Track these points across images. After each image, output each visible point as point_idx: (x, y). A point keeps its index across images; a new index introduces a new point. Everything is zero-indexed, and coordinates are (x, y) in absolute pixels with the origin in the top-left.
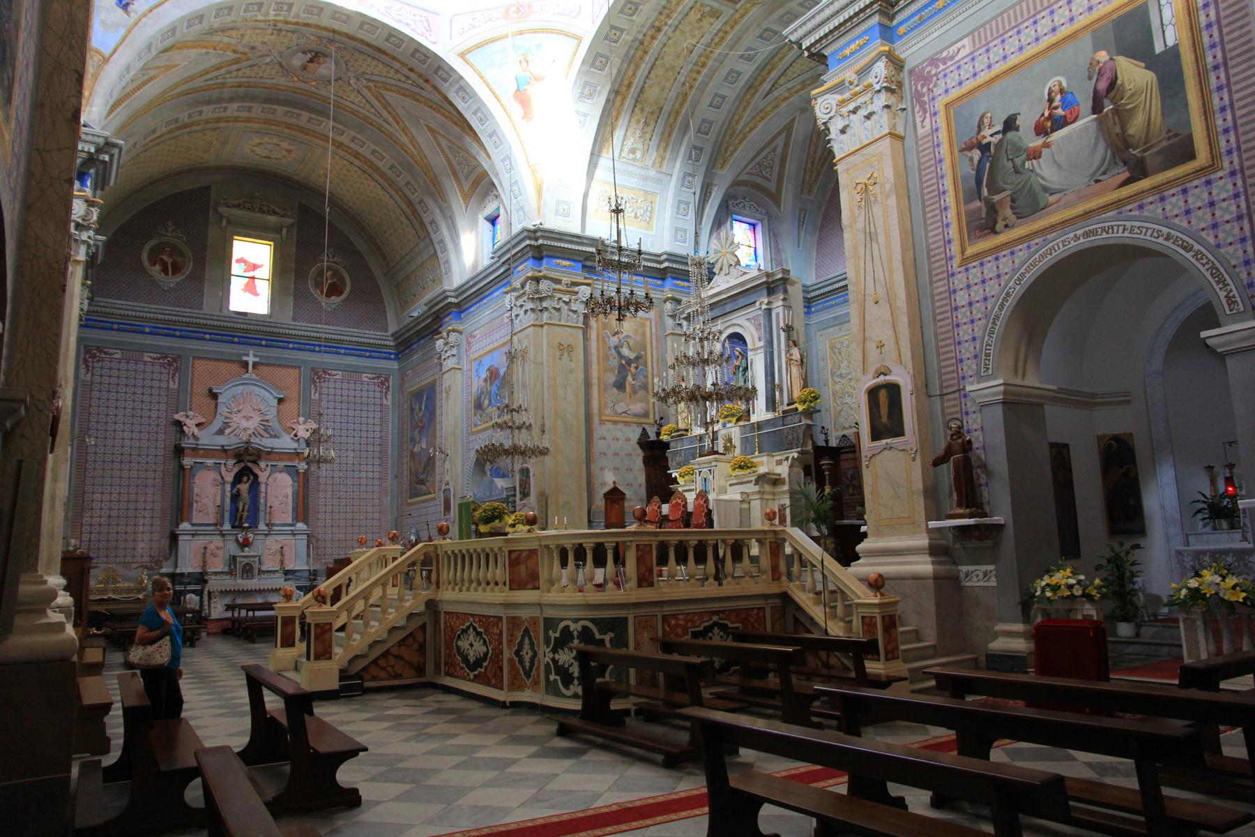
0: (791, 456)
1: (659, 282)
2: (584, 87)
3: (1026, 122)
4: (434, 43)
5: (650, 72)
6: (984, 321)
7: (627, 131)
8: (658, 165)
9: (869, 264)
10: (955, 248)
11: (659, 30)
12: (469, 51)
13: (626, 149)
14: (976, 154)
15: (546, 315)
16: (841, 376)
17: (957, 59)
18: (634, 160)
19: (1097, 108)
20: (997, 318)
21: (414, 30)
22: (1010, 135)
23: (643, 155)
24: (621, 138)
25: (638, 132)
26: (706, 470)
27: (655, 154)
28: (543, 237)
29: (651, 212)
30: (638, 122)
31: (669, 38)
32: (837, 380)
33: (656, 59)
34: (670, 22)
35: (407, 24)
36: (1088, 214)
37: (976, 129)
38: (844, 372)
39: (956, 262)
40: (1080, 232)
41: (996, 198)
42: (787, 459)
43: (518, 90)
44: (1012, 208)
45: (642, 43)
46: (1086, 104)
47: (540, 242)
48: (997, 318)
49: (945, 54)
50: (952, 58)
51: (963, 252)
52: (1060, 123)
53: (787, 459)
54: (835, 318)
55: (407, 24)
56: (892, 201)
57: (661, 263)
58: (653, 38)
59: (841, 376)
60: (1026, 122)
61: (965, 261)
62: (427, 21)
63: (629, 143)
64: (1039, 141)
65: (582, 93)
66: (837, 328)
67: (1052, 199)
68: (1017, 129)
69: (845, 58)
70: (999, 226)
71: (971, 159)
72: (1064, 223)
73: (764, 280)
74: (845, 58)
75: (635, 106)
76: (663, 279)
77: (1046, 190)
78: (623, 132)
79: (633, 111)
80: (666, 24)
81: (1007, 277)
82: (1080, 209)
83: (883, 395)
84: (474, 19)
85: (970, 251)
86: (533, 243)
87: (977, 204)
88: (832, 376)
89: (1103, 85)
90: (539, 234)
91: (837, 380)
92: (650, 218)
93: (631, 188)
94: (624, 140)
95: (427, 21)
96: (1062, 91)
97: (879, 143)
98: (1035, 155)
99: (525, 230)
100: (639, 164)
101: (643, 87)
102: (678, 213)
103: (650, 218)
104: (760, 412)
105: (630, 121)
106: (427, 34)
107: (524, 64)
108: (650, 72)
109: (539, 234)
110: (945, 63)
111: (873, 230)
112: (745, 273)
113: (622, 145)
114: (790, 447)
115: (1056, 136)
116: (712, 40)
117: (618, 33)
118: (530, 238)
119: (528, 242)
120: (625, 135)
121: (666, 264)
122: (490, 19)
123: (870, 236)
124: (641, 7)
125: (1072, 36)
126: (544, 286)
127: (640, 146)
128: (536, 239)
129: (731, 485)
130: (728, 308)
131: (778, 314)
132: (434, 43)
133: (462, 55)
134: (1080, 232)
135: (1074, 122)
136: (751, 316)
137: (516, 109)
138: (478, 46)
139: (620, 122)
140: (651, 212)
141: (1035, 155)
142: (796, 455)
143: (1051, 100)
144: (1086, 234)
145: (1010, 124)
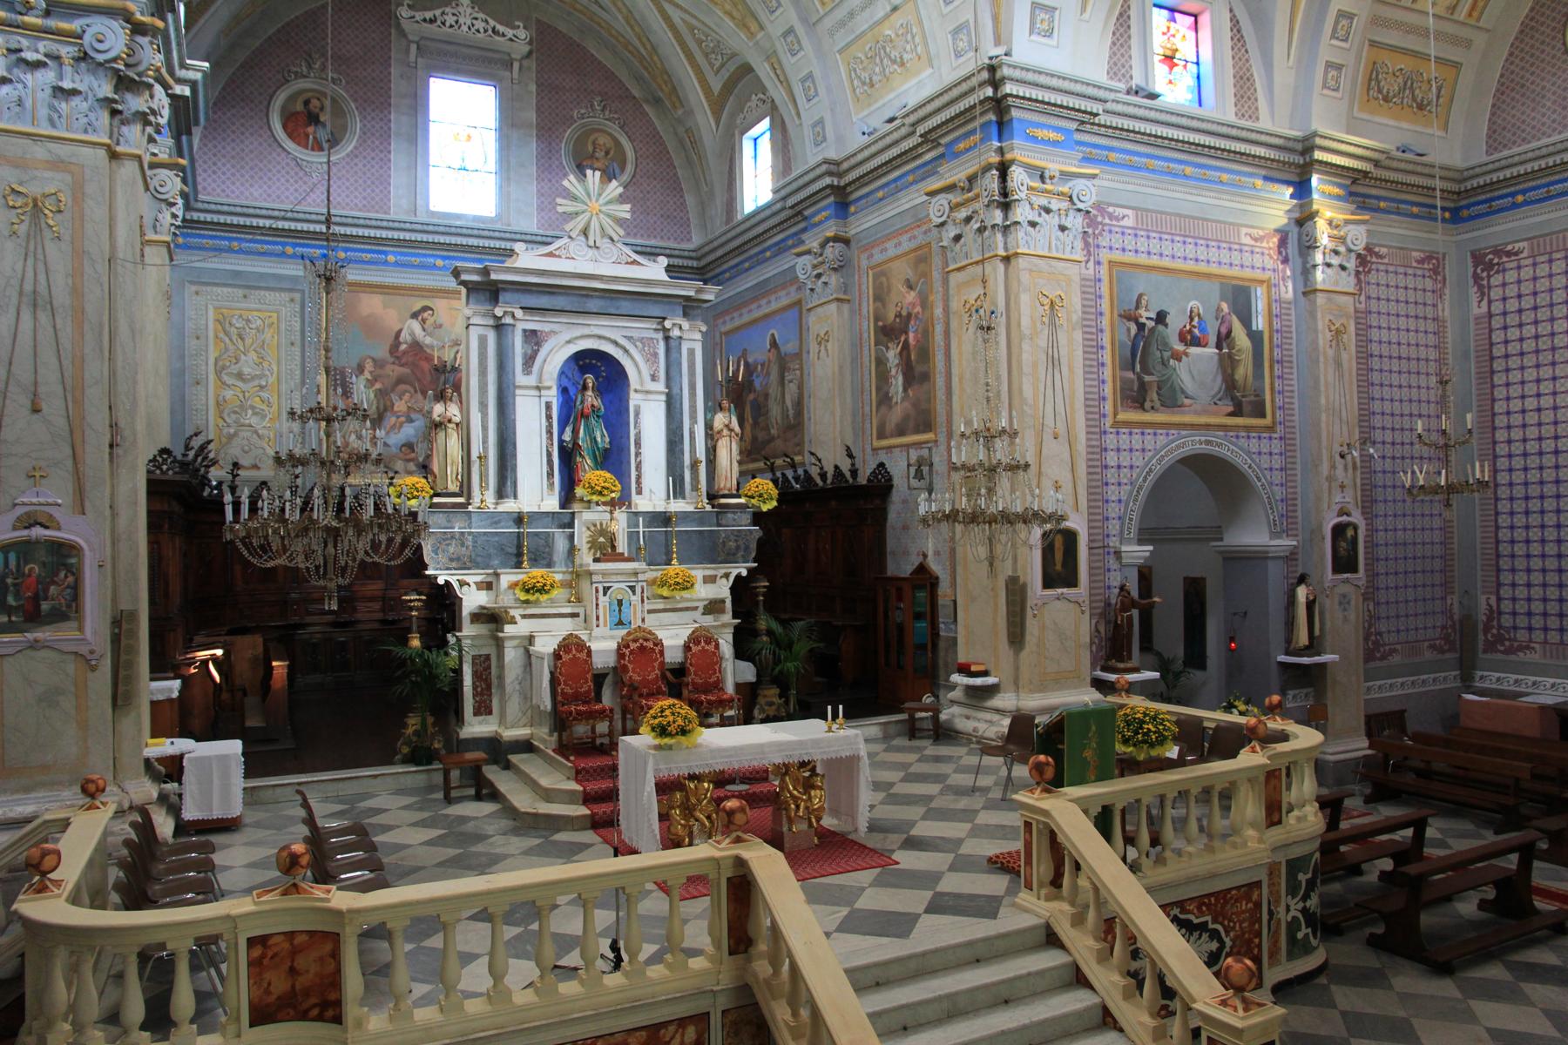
0: (734, 573)
3: (1176, 322)
6: (1128, 487)
9: (1049, 392)
10: (1108, 407)
14: (1134, 329)
16: (240, 376)
17: (1122, 223)
19: (1219, 346)
20: (1140, 488)
22: (1161, 327)
26: (623, 585)
32: (229, 381)
36: (1207, 426)
37: (1134, 304)
38: (246, 370)
39: (1109, 421)
40: (1203, 439)
41: (1147, 378)
42: (727, 576)
44: (1158, 394)
46: (1213, 339)
48: (1140, 488)
49: (1111, 209)
50: (1117, 219)
51: (1115, 414)
52: (1197, 342)
53: (727, 576)
54: (237, 274)
56: (1078, 336)
59: (240, 376)
60: (1176, 322)
61: (1116, 424)
64: (1180, 347)
66: (240, 292)
67: (1187, 401)
68: (1166, 325)
69: (1034, 139)
70: (1147, 405)
71: (1129, 330)
72: (1193, 426)
74: (1034, 139)
77: (1183, 391)
81: (1150, 454)
82: (1203, 420)
83: (1059, 542)
85: (1121, 416)
87: (1130, 375)
88: (218, 373)
89: (1224, 330)
91: (229, 381)
96: (1199, 315)
97: (1069, 265)
98: (1177, 357)
104: (653, 494)
110: (1111, 219)
111: (1056, 356)
114: (730, 558)
115: (1193, 350)
123: (1054, 362)
125: (1208, 276)
129: (650, 612)
130: (593, 305)
131: (691, 352)
134: (1203, 439)
135: (1204, 346)
136: (635, 334)
141: (1177, 357)
142: (744, 573)
143: (1192, 319)
144: (1208, 442)
145: (1161, 318)
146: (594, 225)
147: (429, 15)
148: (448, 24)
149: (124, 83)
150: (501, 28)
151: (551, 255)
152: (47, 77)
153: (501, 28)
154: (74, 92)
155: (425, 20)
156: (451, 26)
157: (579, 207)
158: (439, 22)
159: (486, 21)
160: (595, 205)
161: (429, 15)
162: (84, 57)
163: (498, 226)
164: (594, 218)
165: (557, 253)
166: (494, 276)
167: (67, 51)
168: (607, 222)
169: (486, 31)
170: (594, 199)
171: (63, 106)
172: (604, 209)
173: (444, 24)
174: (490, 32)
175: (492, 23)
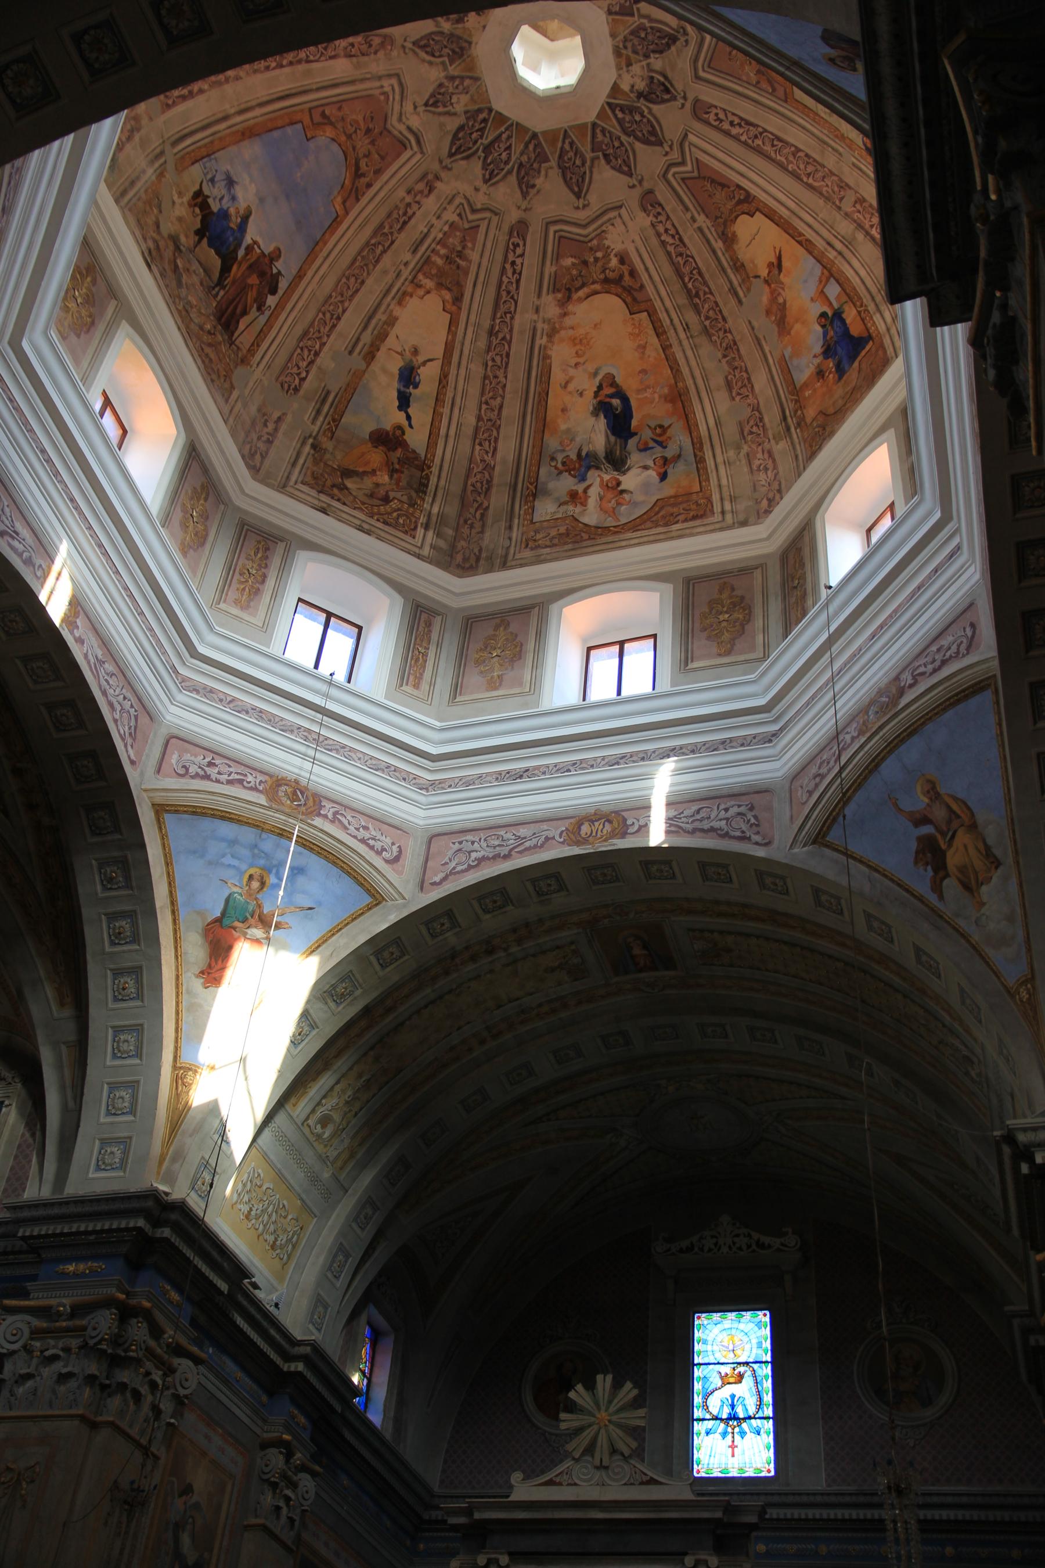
1: (264, 1398)
2: (342, 980)
4: (133, 762)
5: (426, 1006)
7: (337, 1083)
8: (339, 1163)
11: (490, 952)
12: (176, 810)
13: (318, 1114)
15: (115, 1402)
18: (319, 1137)
21: (116, 721)
23: (333, 1136)
24: (323, 1092)
25: (349, 1093)
27: (347, 1142)
28: (176, 1227)
29: (294, 1247)
30: (360, 1076)
31: (491, 971)
33: (450, 992)
34: (514, 949)
35: (111, 705)
43: (218, 921)
45: (453, 957)
47: (166, 1232)
55: (111, 705)
57: (288, 1358)
58: (474, 958)
62: (136, 717)
63: (330, 1103)
65: (334, 987)
73: (718, 1515)
75: (372, 1048)
76: (271, 1394)
78: (331, 1081)
79: (365, 1054)
80: (505, 950)
84: (211, 764)
86: (148, 1228)
90: (174, 1216)
92: (289, 1257)
93: (290, 1188)
94: (324, 1097)
95: (136, 717)
99: (154, 1195)
100: (320, 1148)
101: (402, 1024)
102: (330, 1269)
103: (289, 1257)
105: (351, 1069)
106: (129, 741)
107: (255, 885)
108: (426, 1006)
109: (174, 1216)
112: (652, 1481)
113: (319, 1104)
116: (540, 1005)
117: (447, 925)
118: (147, 1215)
119: (141, 1223)
120: (332, 1089)
121: (300, 1367)
122: (240, 782)
124: (510, 908)
126: (138, 1331)
127: (337, 1117)
128: (157, 1223)
132: (133, 762)
133: (160, 810)
137: (195, 949)
138: (198, 812)
139: (339, 1063)
140: (294, 1247)
146: (602, 1440)
147: (685, 1244)
148: (706, 1249)
149: (116, 1361)
150: (766, 1240)
151: (550, 1483)
152: (59, 1367)
153: (766, 1240)
154: (70, 1375)
155: (681, 1251)
156: (710, 1250)
157: (586, 1419)
158: (696, 1249)
159: (750, 1236)
160: (603, 1415)
161: (685, 1244)
162: (84, 1346)
163: (774, 1488)
164: (603, 1431)
165: (558, 1480)
166: (477, 1516)
167: (74, 1343)
168: (616, 1433)
169: (749, 1246)
170: (603, 1408)
171: (62, 1389)
172: (614, 1418)
173: (702, 1249)
174: (754, 1247)
175: (756, 1236)
